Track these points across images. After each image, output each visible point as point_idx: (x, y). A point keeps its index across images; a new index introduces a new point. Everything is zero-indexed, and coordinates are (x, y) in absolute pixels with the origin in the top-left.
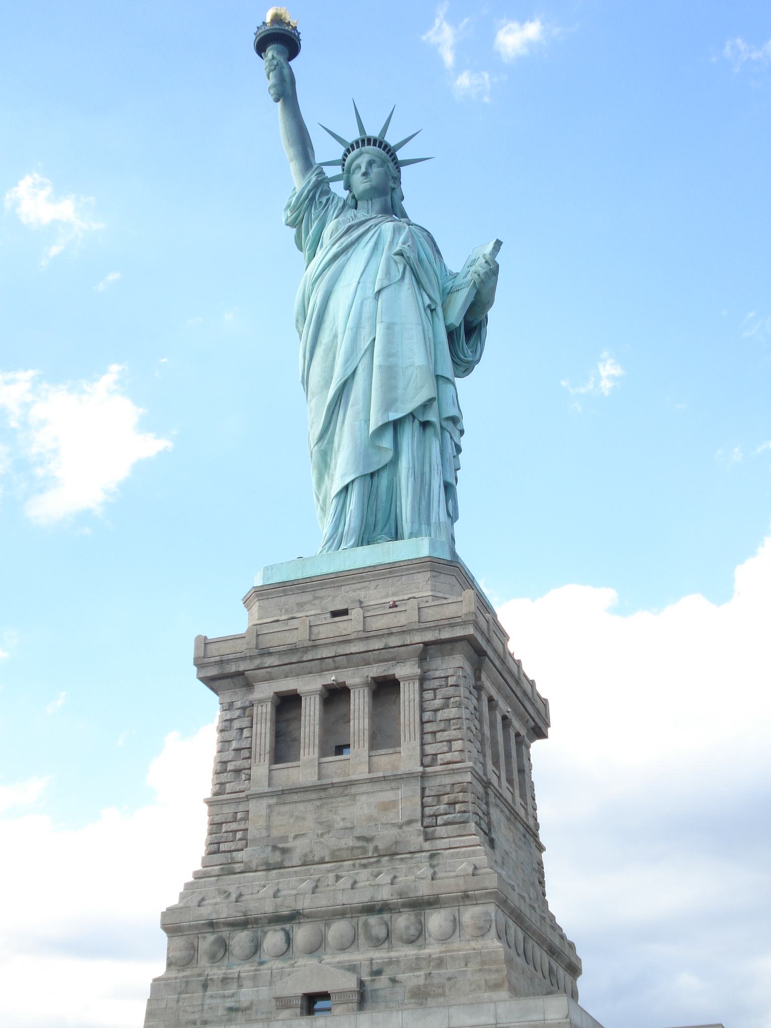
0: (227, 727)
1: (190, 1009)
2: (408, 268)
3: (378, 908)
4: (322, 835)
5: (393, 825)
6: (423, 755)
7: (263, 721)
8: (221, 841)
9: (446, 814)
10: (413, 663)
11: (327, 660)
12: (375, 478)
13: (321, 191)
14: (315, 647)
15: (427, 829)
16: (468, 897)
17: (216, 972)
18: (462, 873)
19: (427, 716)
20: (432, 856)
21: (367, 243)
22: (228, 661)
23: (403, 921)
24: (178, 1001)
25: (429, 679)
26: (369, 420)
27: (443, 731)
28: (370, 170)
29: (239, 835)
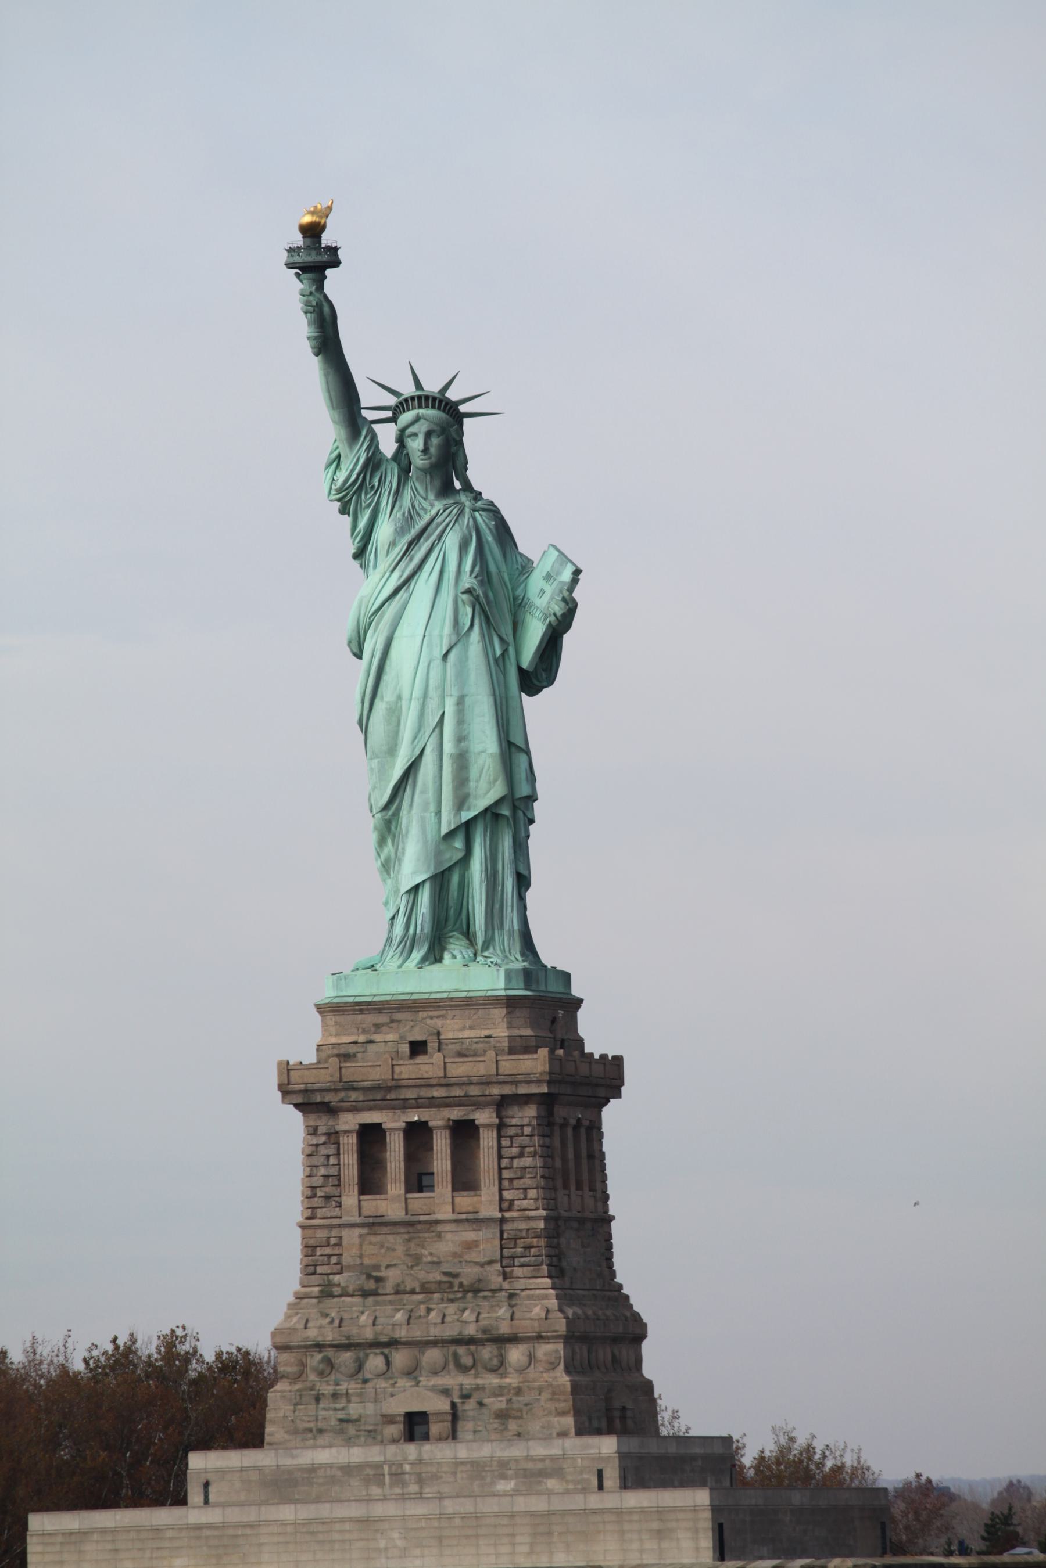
0: (313, 1152)
2: (477, 607)
5: (477, 1263)
6: (501, 1199)
7: (350, 1152)
9: (522, 1257)
10: (491, 1110)
11: (411, 1101)
14: (398, 1087)
18: (537, 1317)
19: (505, 1162)
20: (511, 1296)
22: (313, 1091)
23: (487, 1352)
24: (294, 1411)
26: (440, 812)
29: (334, 1260)
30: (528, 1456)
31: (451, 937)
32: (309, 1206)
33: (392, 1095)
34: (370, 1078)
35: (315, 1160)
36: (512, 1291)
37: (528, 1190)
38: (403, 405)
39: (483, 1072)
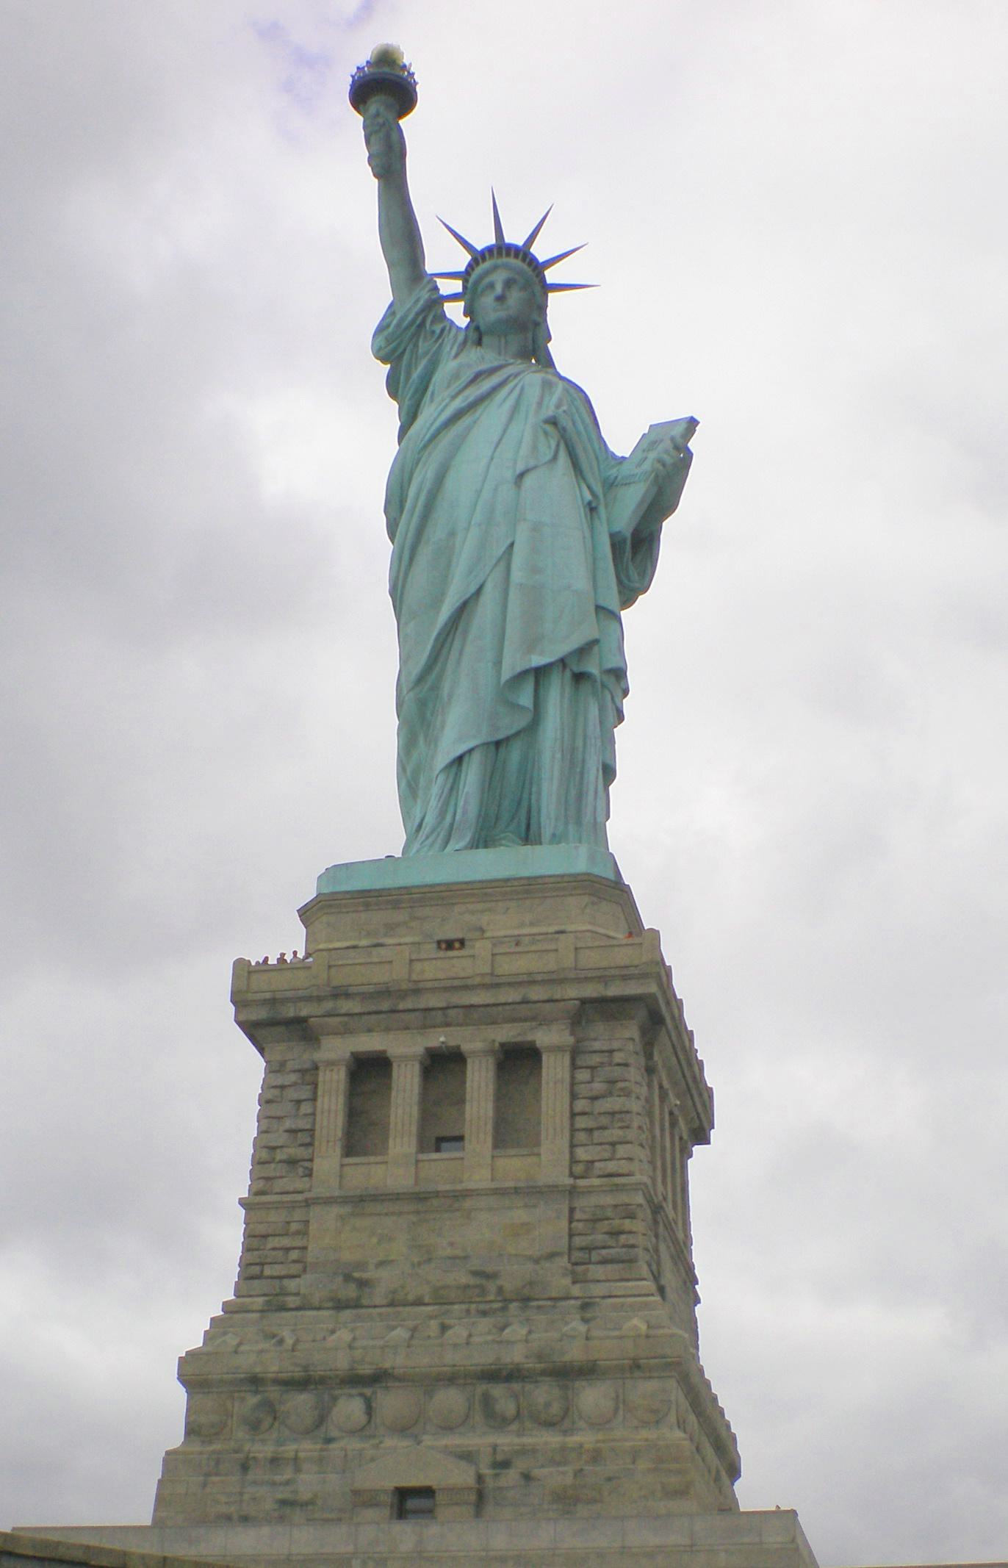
0: (276, 1097)
1: (223, 1499)
2: (562, 447)
3: (504, 1373)
4: (419, 1264)
6: (573, 1161)
8: (266, 1261)
9: (604, 1248)
11: (433, 1013)
12: (502, 750)
13: (434, 317)
14: (417, 991)
15: (575, 1267)
16: (638, 1367)
17: (263, 1450)
19: (581, 1105)
20: (585, 1306)
21: (505, 400)
22: (284, 1001)
23: (543, 1394)
24: (205, 1485)
25: (585, 1052)
27: (604, 1128)
28: (508, 294)
29: (294, 1255)
30: (623, 1547)
31: (504, 838)
32: (263, 1175)
33: (408, 1003)
34: (375, 981)
35: (275, 1110)
36: (587, 1300)
37: (618, 1146)
38: (478, 257)
39: (552, 966)
